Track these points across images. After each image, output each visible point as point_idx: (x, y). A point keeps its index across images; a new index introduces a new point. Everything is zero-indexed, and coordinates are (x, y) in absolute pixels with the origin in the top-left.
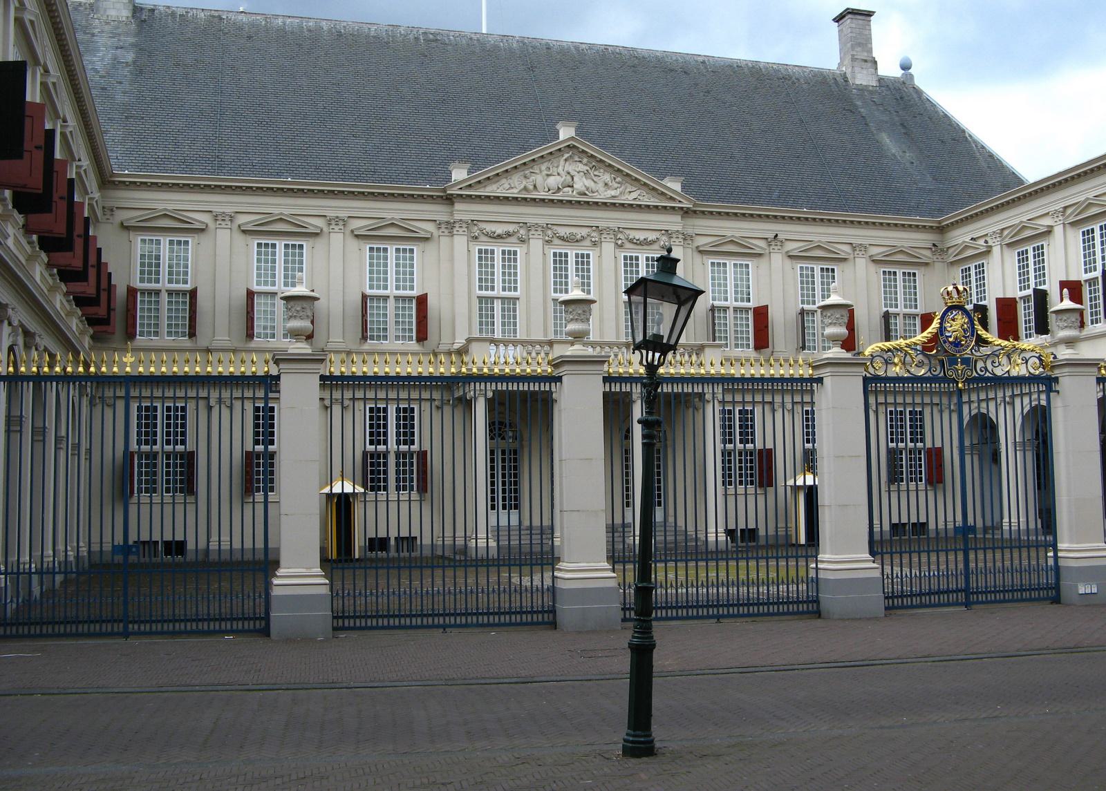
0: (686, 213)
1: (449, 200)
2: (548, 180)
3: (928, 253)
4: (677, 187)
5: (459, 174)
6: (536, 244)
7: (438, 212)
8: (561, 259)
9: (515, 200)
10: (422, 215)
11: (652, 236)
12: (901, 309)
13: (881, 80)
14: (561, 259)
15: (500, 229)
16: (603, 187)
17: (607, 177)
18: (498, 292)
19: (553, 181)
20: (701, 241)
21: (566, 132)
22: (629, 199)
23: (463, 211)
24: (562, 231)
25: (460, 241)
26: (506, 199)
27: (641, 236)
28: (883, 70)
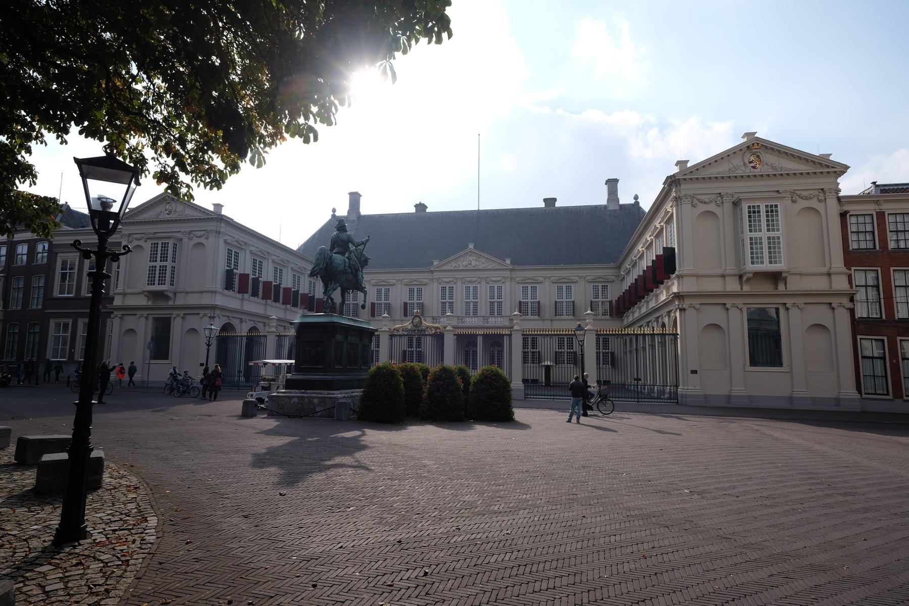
0: (512, 270)
1: (432, 272)
2: (462, 263)
3: (613, 277)
4: (508, 261)
5: (436, 263)
6: (459, 284)
7: (429, 276)
8: (468, 288)
9: (452, 271)
10: (423, 277)
11: (499, 279)
12: (600, 299)
13: (622, 206)
14: (468, 288)
15: (447, 280)
16: (482, 264)
17: (483, 260)
18: (447, 300)
19: (465, 263)
20: (518, 279)
21: (471, 246)
22: (490, 267)
23: (436, 275)
24: (468, 279)
25: (435, 284)
26: (449, 271)
27: (495, 279)
28: (621, 202)
